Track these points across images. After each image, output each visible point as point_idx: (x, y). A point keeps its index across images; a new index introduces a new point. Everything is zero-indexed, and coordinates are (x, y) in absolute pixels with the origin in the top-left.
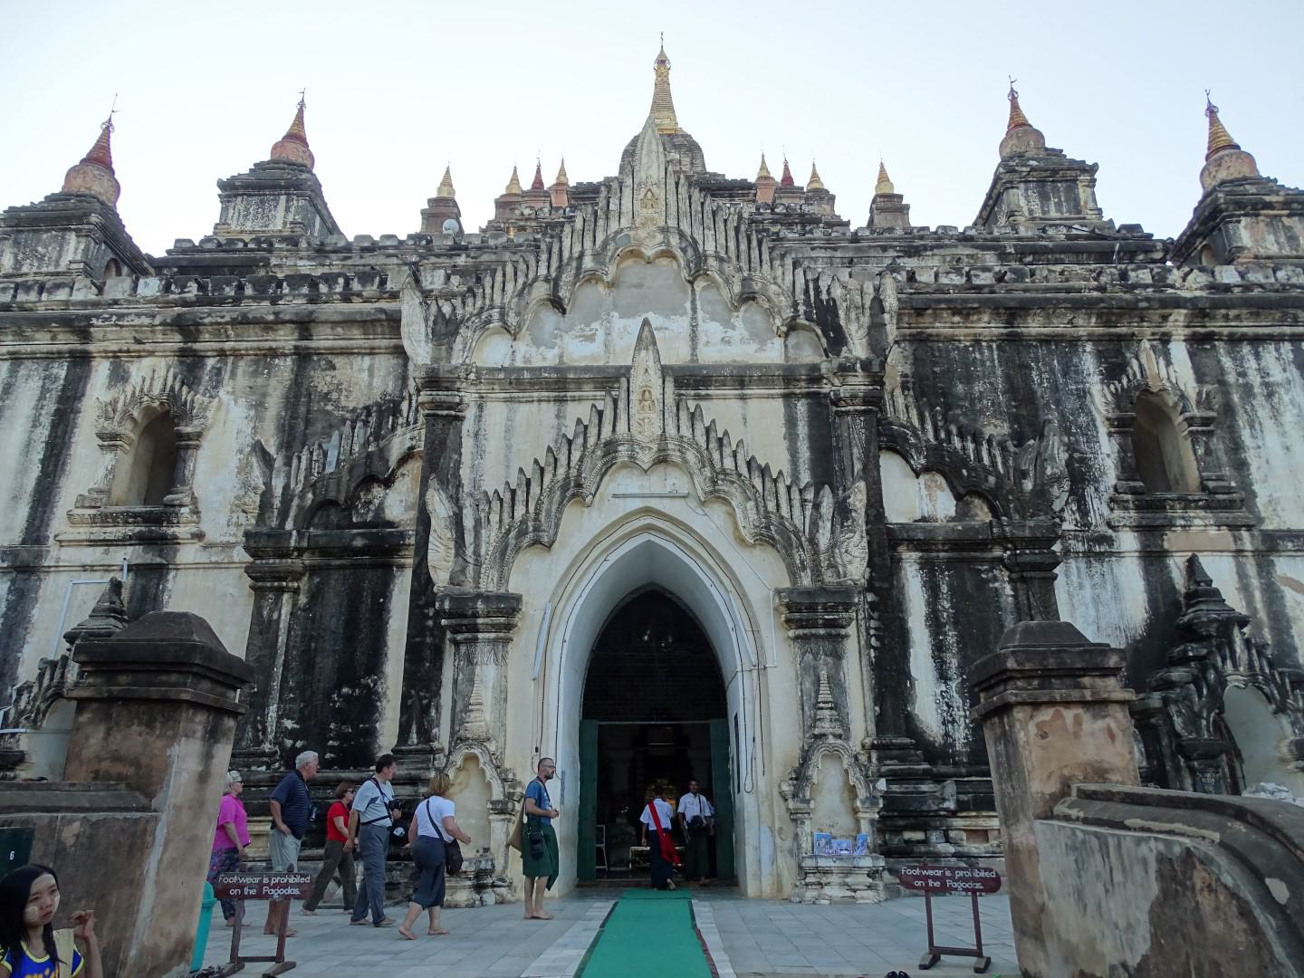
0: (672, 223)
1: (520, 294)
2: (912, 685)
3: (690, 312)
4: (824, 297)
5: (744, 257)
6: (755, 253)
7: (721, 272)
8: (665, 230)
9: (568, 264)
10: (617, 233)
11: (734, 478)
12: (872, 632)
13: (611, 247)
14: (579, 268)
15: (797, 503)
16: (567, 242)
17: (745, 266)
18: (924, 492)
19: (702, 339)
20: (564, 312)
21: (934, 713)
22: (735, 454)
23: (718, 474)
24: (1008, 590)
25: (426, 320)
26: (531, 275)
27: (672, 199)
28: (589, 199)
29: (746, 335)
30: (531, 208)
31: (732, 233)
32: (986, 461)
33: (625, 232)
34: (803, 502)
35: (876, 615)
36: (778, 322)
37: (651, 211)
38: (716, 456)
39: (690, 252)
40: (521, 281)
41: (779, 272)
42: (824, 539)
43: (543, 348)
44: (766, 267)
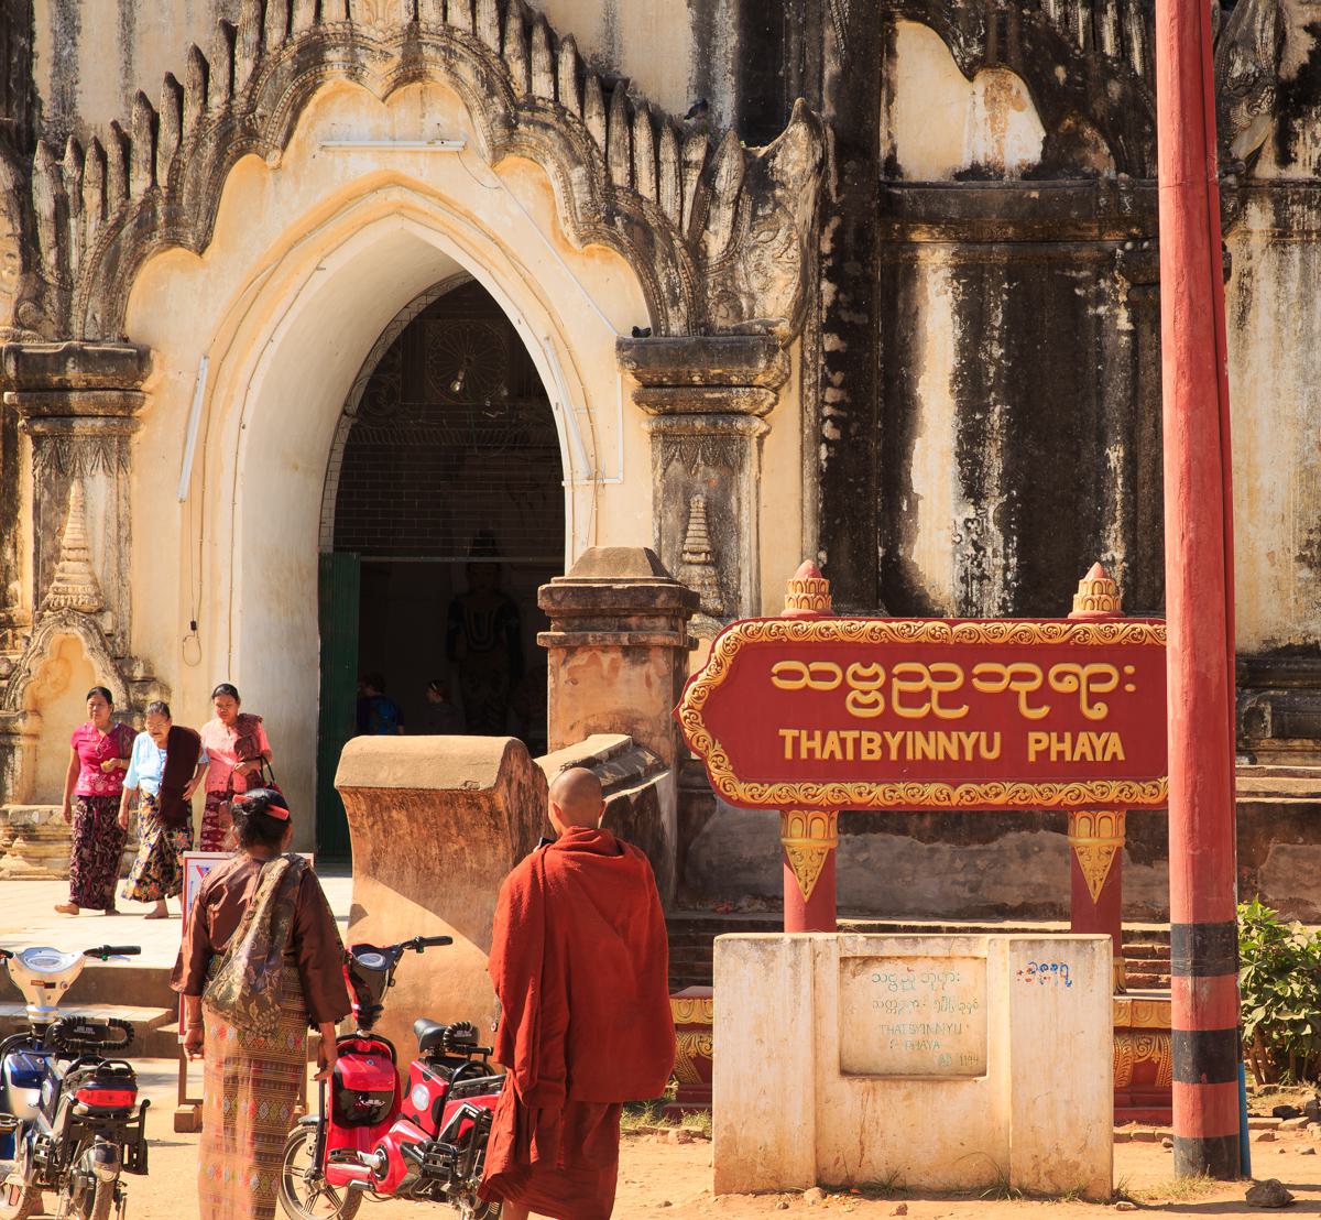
2: (913, 508)
11: (550, 118)
12: (827, 411)
15: (669, 170)
18: (982, 112)
21: (948, 560)
22: (554, 69)
23: (518, 107)
24: (1123, 322)
32: (1109, 48)
34: (683, 165)
35: (837, 378)
38: (517, 69)
42: (716, 244)
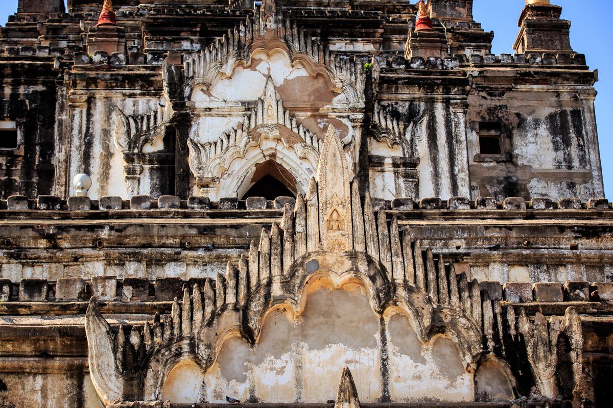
0: (360, 248)
1: (210, 324)
3: (379, 344)
4: (513, 332)
5: (432, 285)
6: (444, 283)
7: (411, 303)
8: (353, 256)
9: (257, 291)
10: (304, 257)
13: (300, 273)
14: (267, 296)
16: (253, 267)
17: (432, 295)
19: (393, 375)
20: (253, 342)
25: (115, 351)
26: (219, 303)
27: (358, 220)
28: (170, 33)
29: (437, 370)
30: (103, 54)
31: (419, 261)
33: (313, 257)
36: (468, 359)
37: (338, 233)
39: (379, 281)
40: (209, 309)
41: (468, 305)
43: (233, 382)
44: (455, 299)
